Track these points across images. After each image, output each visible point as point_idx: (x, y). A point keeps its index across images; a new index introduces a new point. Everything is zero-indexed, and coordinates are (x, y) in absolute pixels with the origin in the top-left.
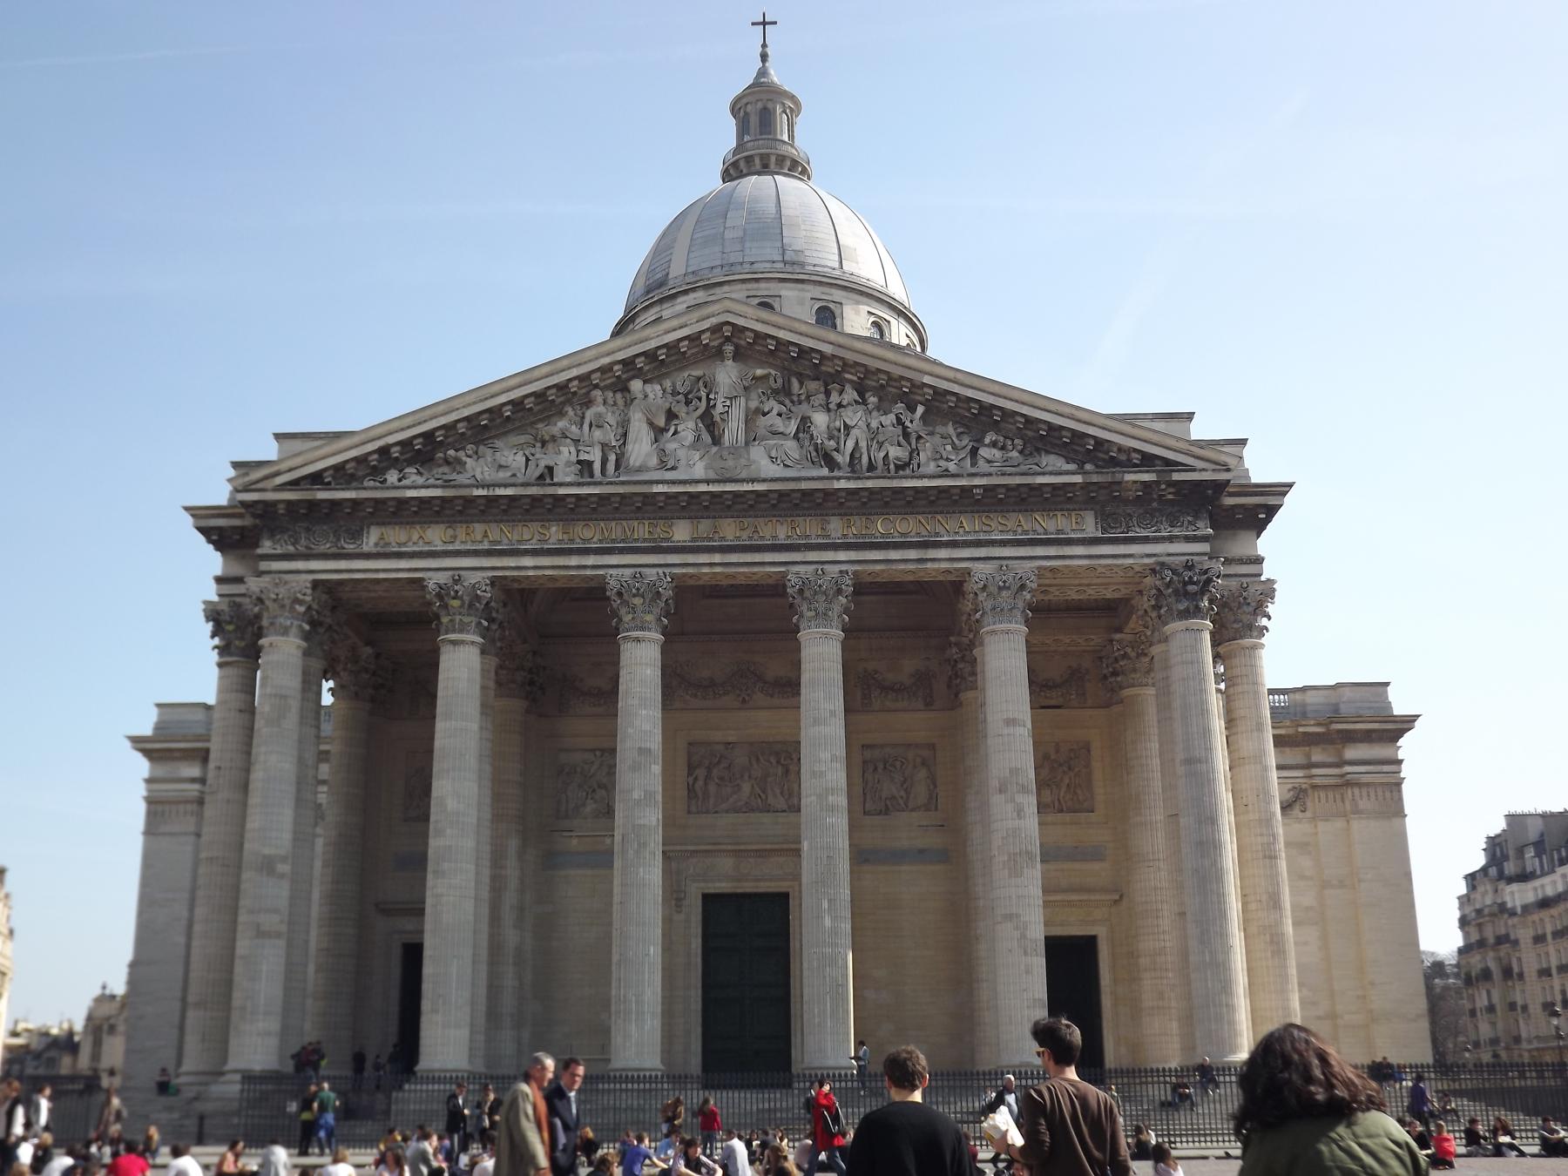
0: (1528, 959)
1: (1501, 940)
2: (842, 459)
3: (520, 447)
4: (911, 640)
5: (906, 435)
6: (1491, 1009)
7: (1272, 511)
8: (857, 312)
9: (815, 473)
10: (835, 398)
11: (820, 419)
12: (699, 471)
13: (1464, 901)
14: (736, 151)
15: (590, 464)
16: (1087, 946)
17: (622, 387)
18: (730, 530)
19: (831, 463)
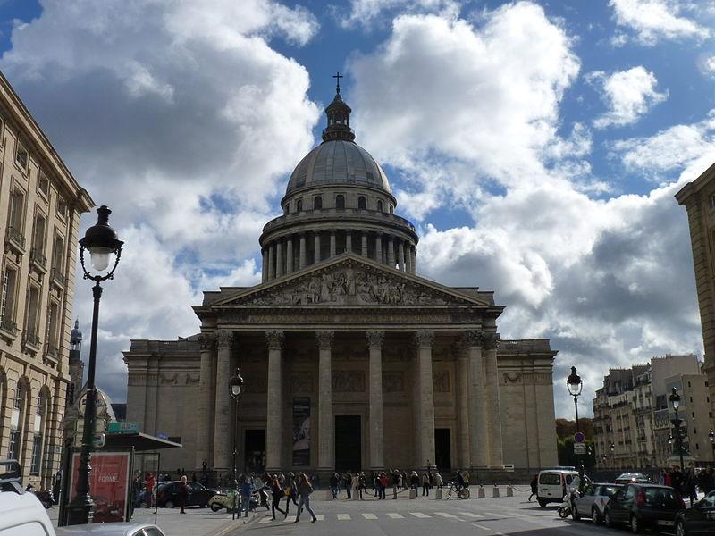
0: (615, 426)
1: (607, 417)
2: (382, 299)
3: (291, 293)
4: (401, 347)
5: (399, 292)
6: (602, 443)
7: (500, 313)
8: (373, 198)
9: (374, 303)
10: (380, 281)
11: (376, 287)
12: (342, 302)
13: (595, 401)
14: (327, 129)
15: (311, 299)
16: (447, 431)
17: (320, 276)
18: (351, 320)
19: (378, 299)
